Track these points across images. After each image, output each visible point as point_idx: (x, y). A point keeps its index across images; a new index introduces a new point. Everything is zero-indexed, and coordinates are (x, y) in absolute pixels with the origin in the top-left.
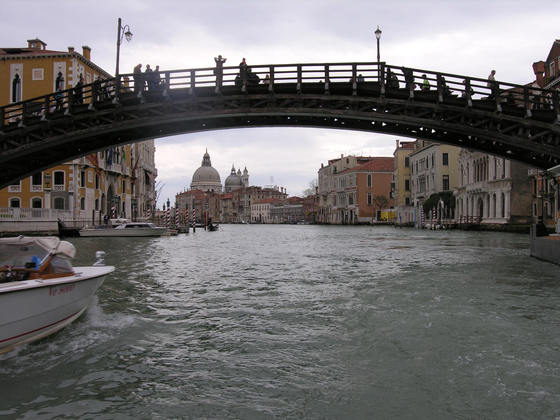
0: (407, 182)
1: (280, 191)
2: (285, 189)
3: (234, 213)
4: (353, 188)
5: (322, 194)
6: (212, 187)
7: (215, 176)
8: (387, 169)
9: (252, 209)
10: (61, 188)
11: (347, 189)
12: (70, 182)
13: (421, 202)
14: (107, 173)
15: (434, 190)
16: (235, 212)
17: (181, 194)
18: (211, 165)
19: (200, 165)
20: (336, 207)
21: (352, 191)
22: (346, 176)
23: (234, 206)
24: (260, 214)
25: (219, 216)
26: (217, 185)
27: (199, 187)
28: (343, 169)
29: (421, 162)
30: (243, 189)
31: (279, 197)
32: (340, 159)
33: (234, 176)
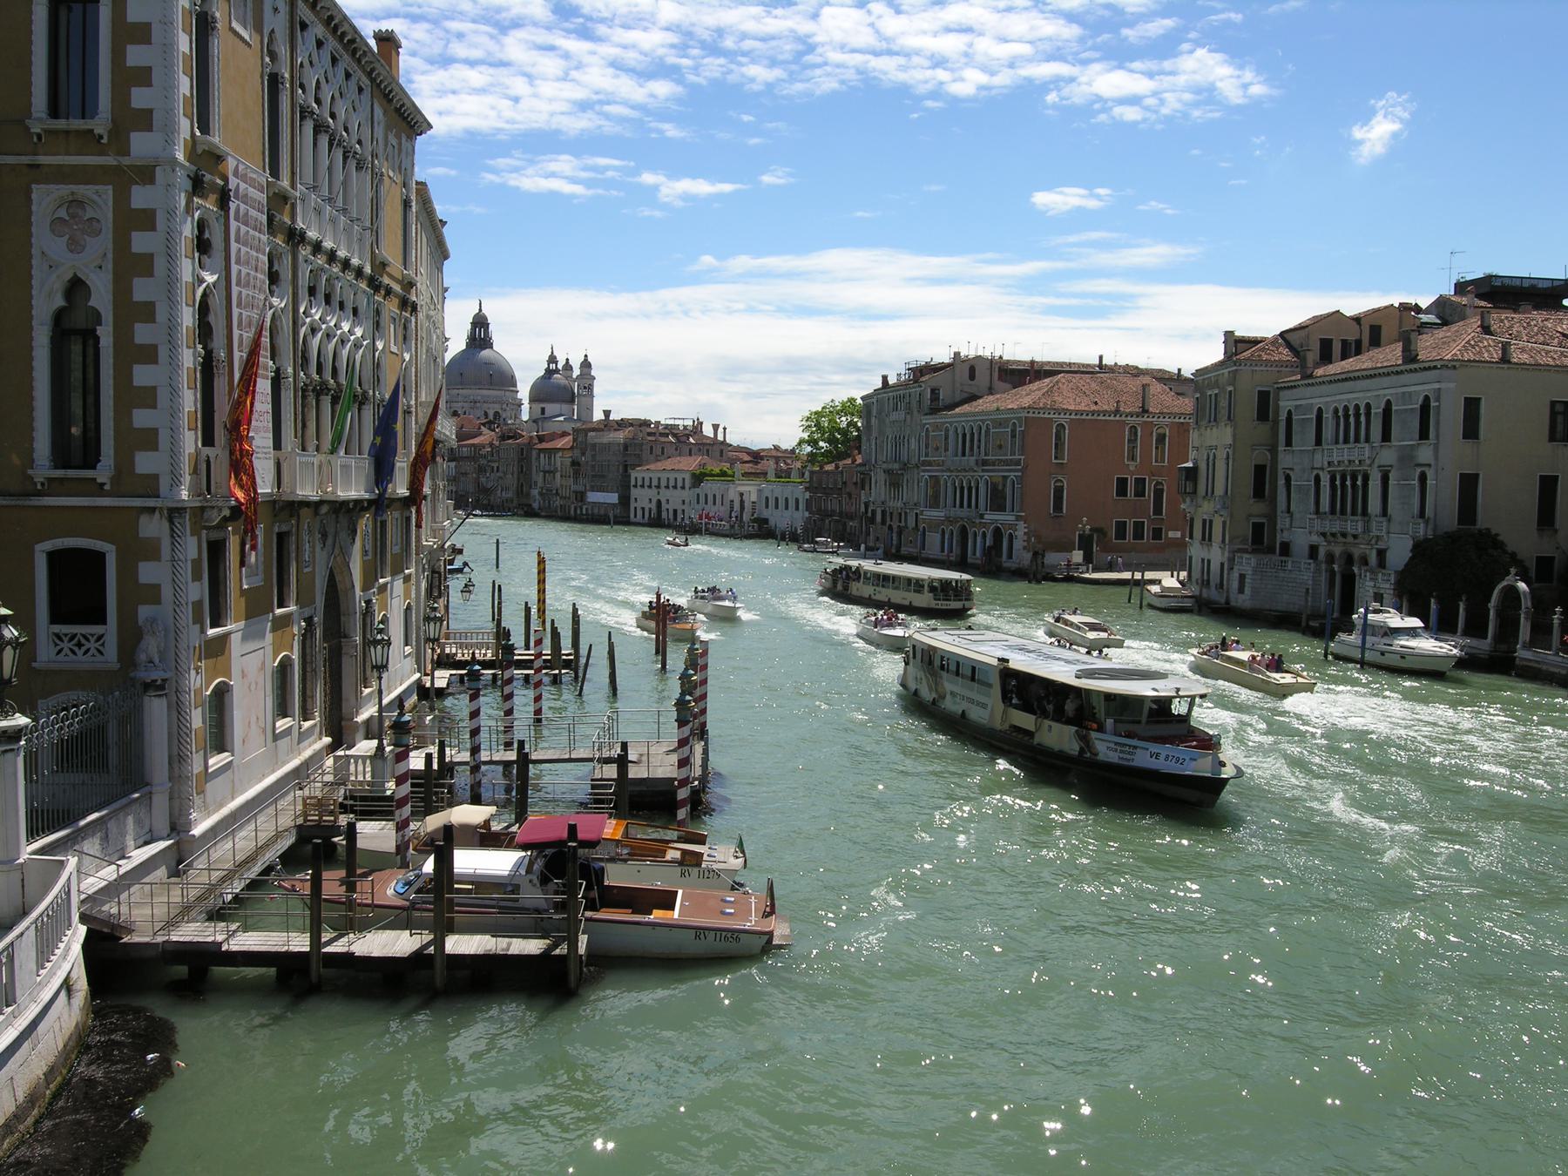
0: (1260, 471)
1: (708, 431)
2: (725, 429)
3: (576, 492)
4: (1007, 463)
5: (885, 466)
7: (502, 378)
8: (1113, 409)
9: (633, 483)
10: (92, 645)
11: (985, 463)
12: (144, 611)
13: (1337, 550)
14: (324, 509)
15: (1427, 522)
16: (580, 488)
18: (491, 346)
20: (942, 514)
21: (999, 471)
22: (982, 421)
23: (576, 474)
24: (659, 502)
25: (528, 494)
28: (958, 398)
29: (1347, 416)
30: (605, 426)
31: (708, 451)
32: (949, 365)
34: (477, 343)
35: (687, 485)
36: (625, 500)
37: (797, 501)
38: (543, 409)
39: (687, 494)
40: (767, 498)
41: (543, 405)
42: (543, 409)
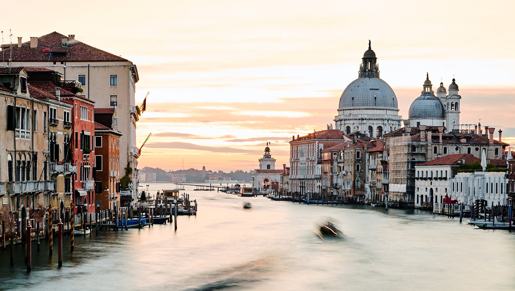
2: (500, 132)
3: (384, 184)
6: (380, 122)
9: (416, 176)
16: (386, 182)
17: (299, 139)
18: (377, 75)
19: (355, 75)
24: (431, 190)
25: (363, 187)
26: (390, 117)
27: (351, 122)
30: (404, 132)
33: (428, 99)
34: (367, 73)
35: (448, 177)
36: (411, 190)
37: (502, 184)
38: (418, 124)
39: (446, 184)
40: (487, 183)
41: (418, 121)
42: (418, 124)
